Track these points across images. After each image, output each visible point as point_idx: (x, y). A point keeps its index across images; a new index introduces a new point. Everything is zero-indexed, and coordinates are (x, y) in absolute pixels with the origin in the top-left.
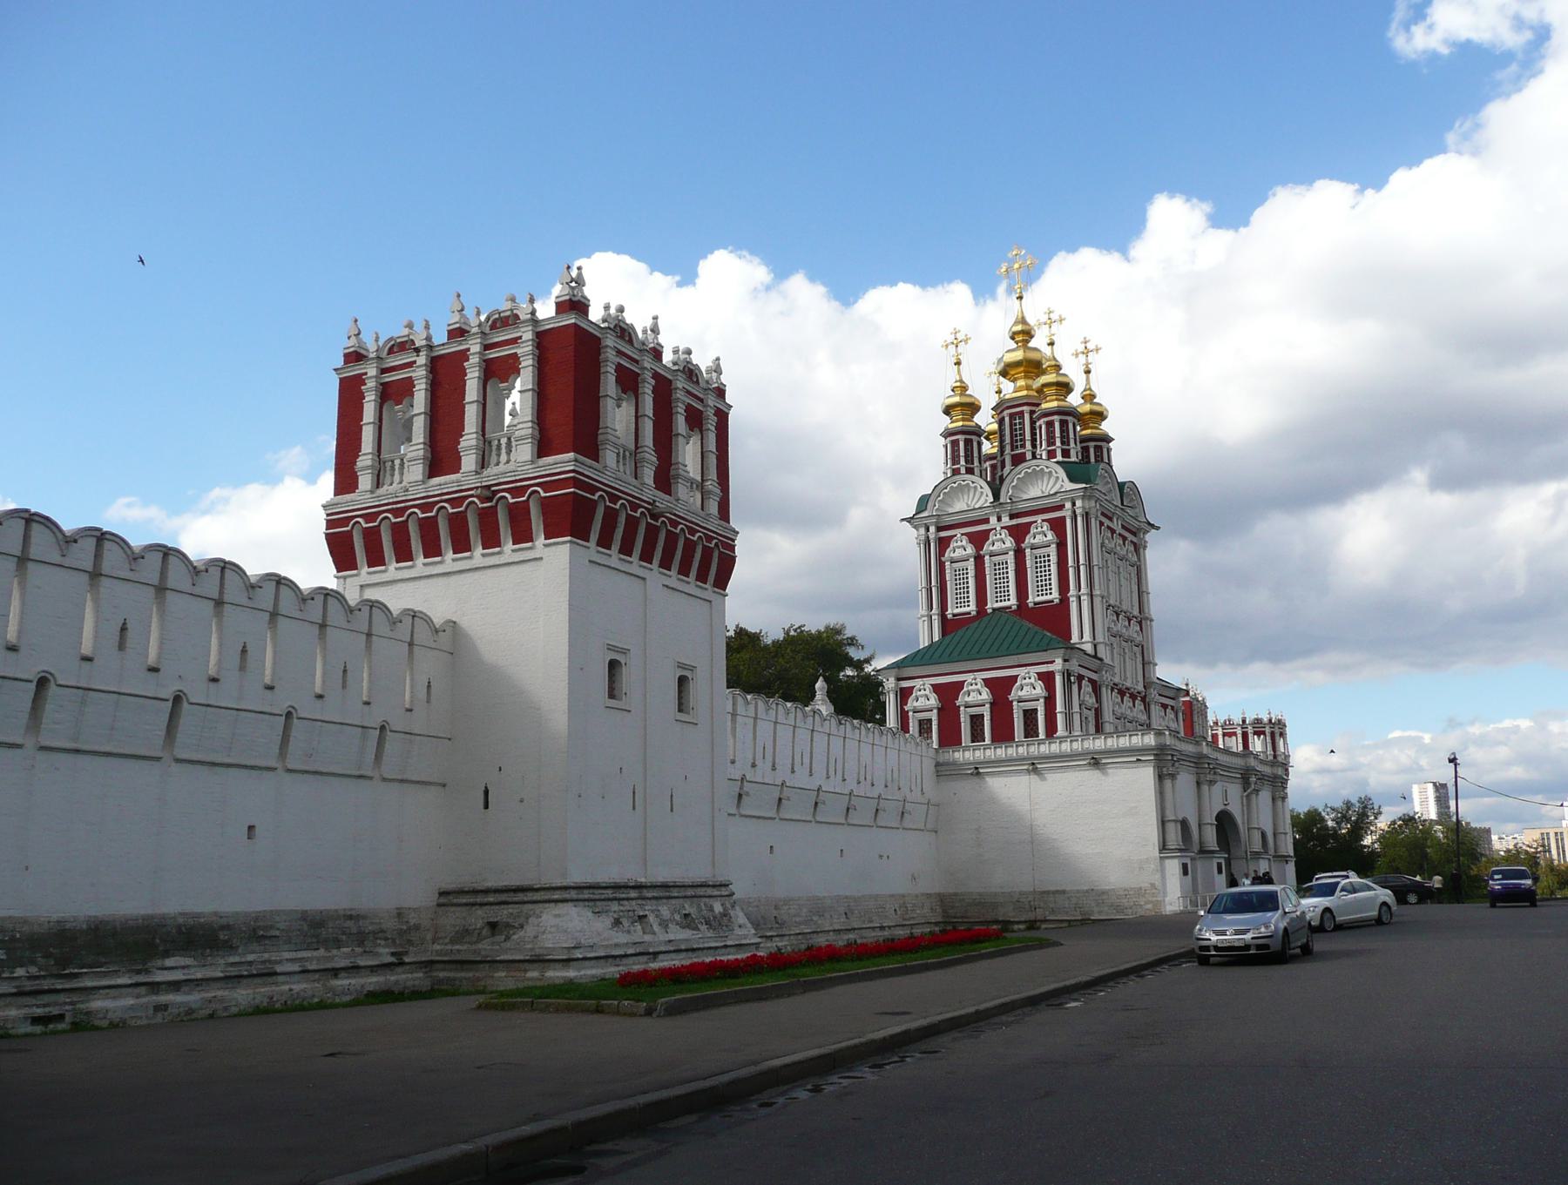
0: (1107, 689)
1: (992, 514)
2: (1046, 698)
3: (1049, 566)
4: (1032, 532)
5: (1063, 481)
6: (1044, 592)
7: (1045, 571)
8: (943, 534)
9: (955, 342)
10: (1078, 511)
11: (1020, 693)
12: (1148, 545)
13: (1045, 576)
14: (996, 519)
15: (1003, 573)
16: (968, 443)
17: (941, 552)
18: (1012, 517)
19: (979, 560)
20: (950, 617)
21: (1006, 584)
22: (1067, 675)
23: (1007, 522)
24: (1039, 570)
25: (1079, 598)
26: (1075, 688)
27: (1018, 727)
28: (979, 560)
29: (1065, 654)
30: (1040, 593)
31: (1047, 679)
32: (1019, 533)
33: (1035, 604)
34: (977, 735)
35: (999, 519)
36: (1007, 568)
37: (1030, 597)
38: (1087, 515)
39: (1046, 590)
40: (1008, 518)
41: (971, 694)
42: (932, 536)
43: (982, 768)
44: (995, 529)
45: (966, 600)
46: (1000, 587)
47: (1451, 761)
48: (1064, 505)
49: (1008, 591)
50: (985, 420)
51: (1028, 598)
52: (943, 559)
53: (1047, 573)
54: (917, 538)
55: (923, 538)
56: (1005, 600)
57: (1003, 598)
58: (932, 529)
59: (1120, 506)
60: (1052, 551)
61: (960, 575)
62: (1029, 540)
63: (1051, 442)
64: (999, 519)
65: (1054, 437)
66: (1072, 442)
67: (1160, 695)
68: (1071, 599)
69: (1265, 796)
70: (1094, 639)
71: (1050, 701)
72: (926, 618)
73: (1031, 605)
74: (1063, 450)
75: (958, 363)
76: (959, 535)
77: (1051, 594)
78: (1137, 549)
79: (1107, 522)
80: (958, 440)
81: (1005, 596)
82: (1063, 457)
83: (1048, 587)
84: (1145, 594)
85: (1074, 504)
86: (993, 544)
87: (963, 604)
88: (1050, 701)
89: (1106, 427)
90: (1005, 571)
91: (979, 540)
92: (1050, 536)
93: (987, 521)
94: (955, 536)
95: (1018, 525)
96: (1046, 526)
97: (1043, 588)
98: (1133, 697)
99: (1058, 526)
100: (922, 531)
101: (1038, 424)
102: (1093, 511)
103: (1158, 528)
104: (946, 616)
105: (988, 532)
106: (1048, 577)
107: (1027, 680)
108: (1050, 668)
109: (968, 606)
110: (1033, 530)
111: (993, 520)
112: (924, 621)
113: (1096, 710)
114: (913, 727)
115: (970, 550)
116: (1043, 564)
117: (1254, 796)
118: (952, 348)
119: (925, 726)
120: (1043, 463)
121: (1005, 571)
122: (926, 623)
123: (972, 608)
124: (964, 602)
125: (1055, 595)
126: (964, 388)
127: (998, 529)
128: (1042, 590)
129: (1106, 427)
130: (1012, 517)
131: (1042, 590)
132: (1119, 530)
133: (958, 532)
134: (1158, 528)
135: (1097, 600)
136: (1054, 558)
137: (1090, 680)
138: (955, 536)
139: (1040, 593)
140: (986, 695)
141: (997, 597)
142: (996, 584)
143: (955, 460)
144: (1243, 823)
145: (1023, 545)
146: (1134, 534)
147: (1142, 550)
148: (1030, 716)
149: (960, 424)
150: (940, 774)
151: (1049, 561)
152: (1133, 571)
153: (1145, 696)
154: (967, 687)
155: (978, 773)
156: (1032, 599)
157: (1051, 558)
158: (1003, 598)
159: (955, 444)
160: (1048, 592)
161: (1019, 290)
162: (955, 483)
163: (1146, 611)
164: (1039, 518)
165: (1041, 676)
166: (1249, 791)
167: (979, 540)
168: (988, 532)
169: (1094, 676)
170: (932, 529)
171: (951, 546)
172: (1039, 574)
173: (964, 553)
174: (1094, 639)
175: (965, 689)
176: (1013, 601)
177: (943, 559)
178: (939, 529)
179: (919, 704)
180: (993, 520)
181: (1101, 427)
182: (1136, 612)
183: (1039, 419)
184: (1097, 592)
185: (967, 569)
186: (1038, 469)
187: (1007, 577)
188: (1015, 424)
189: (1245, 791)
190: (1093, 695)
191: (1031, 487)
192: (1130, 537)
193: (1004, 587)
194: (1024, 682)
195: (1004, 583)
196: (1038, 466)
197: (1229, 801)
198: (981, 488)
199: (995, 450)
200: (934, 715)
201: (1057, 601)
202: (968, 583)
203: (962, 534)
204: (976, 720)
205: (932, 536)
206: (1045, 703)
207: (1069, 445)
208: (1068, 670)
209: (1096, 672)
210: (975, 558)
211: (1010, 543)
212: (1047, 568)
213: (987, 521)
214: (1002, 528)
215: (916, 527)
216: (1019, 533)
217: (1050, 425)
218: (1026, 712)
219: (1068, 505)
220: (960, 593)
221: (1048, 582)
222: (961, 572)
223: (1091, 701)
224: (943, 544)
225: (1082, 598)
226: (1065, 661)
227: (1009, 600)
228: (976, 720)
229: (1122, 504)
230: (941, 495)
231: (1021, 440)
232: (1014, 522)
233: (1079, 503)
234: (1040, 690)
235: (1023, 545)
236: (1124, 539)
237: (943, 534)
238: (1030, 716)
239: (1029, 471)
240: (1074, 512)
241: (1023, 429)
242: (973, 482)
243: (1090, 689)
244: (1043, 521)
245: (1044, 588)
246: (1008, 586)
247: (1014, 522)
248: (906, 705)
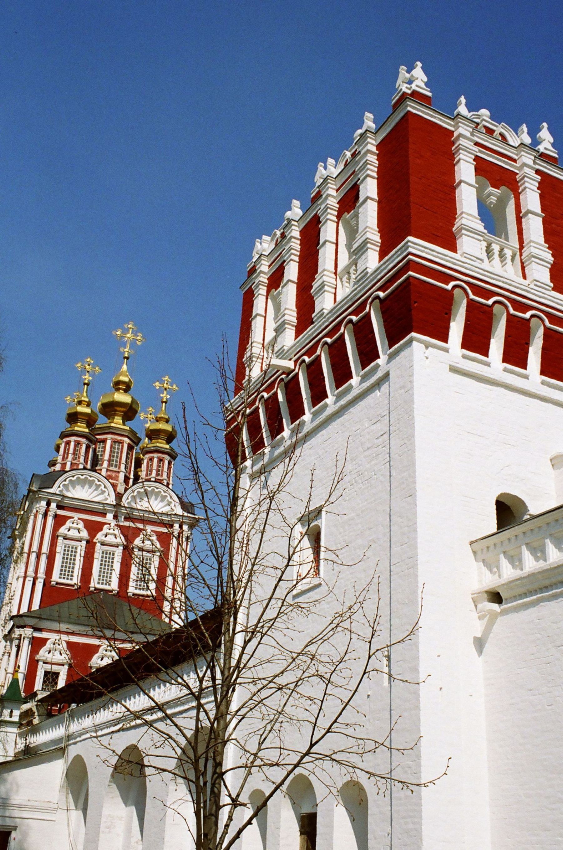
1: (110, 512)
8: (61, 512)
17: (56, 528)
44: (110, 524)
58: (53, 505)
61: (69, 554)
76: (76, 518)
93: (104, 515)
94: (73, 518)
99: (165, 539)
105: (102, 524)
111: (110, 516)
127: (113, 524)
138: (73, 518)
162: (82, 475)
168: (102, 524)
170: (53, 505)
173: (78, 534)
178: (59, 507)
180: (110, 516)
186: (156, 490)
198: (105, 487)
203: (79, 519)
219: (176, 526)
232: (127, 524)
237: (61, 512)
247: (127, 524)
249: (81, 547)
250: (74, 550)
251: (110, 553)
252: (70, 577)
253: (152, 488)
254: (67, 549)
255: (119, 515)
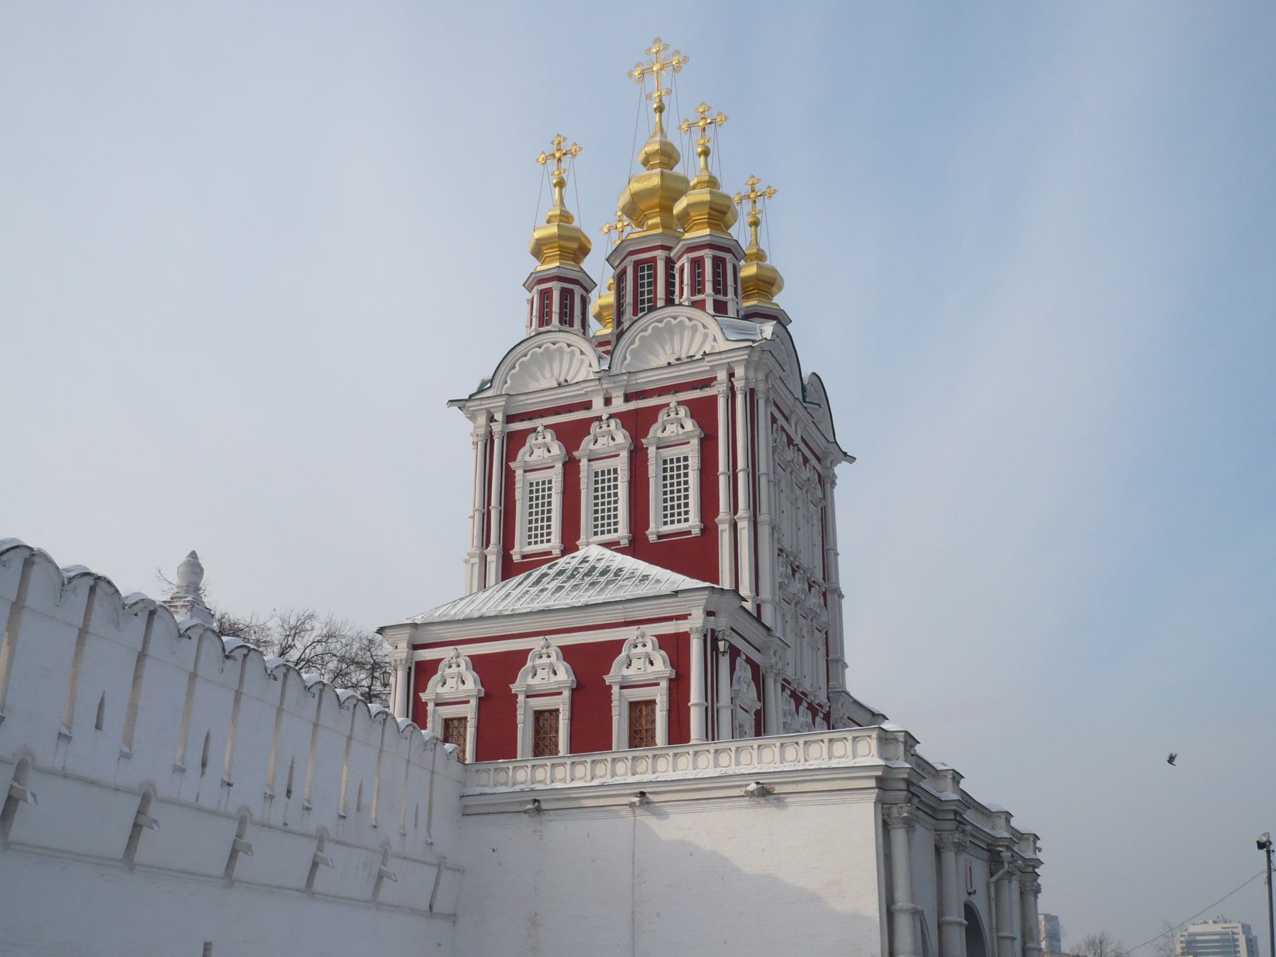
0: (775, 681)
2: (671, 680)
3: (686, 475)
4: (660, 420)
5: (715, 340)
6: (676, 518)
7: (679, 483)
9: (557, 155)
10: (739, 384)
11: (626, 672)
12: (837, 481)
13: (679, 491)
14: (601, 401)
15: (609, 488)
16: (566, 295)
18: (628, 398)
19: (571, 467)
20: (516, 558)
21: (612, 506)
22: (711, 639)
23: (620, 406)
24: (668, 482)
25: (735, 527)
26: (724, 662)
27: (618, 738)
28: (571, 467)
29: (708, 602)
30: (669, 519)
31: (675, 647)
32: (637, 424)
33: (660, 537)
34: (544, 745)
35: (608, 401)
36: (616, 479)
37: (652, 524)
38: (751, 394)
39: (679, 514)
40: (622, 399)
41: (539, 672)
42: (497, 428)
43: (547, 801)
45: (545, 531)
46: (603, 511)
47: (1261, 845)
48: (716, 377)
49: (615, 516)
50: (597, 268)
51: (647, 527)
52: (512, 465)
53: (682, 487)
54: (472, 434)
55: (482, 431)
56: (609, 531)
57: (606, 528)
58: (499, 416)
59: (801, 401)
60: (692, 452)
62: (655, 431)
63: (697, 287)
64: (608, 401)
65: (702, 283)
66: (730, 290)
67: (849, 718)
68: (721, 527)
69: (1012, 890)
70: (757, 594)
71: (678, 687)
72: (476, 560)
73: (652, 538)
74: (716, 302)
75: (561, 184)
77: (686, 520)
78: (821, 480)
79: (781, 421)
80: (549, 291)
81: (609, 524)
82: (714, 310)
83: (683, 510)
84: (832, 553)
85: (731, 375)
86: (596, 441)
87: (539, 539)
88: (678, 687)
89: (781, 300)
90: (612, 484)
91: (572, 435)
92: (690, 425)
93: (587, 405)
95: (637, 412)
96: (683, 411)
97: (674, 509)
98: (814, 710)
99: (703, 412)
100: (482, 420)
101: (677, 266)
102: (761, 388)
103: (852, 459)
104: (511, 556)
106: (682, 494)
107: (640, 649)
108: (682, 626)
109: (549, 541)
110: (662, 416)
111: (598, 403)
112: (473, 565)
113: (758, 713)
114: (433, 729)
115: (557, 449)
116: (675, 473)
117: (1006, 882)
118: (552, 164)
119: (451, 728)
120: (683, 312)
121: (612, 484)
122: (476, 568)
123: (555, 544)
124: (542, 535)
125: (693, 523)
126: (565, 217)
128: (672, 515)
129: (781, 300)
130: (628, 398)
131: (672, 515)
132: (797, 440)
133: (539, 423)
134: (852, 459)
135: (764, 531)
136: (694, 463)
137: (749, 660)
139: (669, 519)
140: (564, 675)
141: (596, 526)
142: (596, 505)
143: (544, 319)
144: (991, 928)
145: (643, 441)
146: (819, 460)
147: (828, 485)
148: (642, 711)
149: (558, 264)
150: (468, 811)
151: (686, 467)
152: (815, 512)
153: (829, 713)
154: (533, 660)
155: (539, 810)
156: (656, 528)
157: (690, 462)
158: (606, 528)
159: (545, 295)
160: (683, 517)
161: (657, 100)
163: (833, 580)
164: (671, 399)
165: (665, 642)
166: (1000, 873)
167: (572, 435)
169: (755, 656)
171: (527, 444)
172: (668, 489)
174: (757, 594)
175: (529, 664)
176: (622, 533)
177: (512, 465)
178: (510, 419)
179: (447, 691)
180: (598, 403)
181: (773, 301)
182: (819, 576)
183: (679, 258)
184: (763, 517)
185: (550, 482)
186: (674, 322)
187: (616, 495)
188: (642, 277)
189: (992, 875)
190: (753, 685)
191: (659, 348)
192: (814, 462)
193: (609, 510)
194: (634, 651)
195: (609, 503)
196: (675, 318)
197: (974, 888)
198: (582, 353)
199: (608, 331)
200: (469, 711)
201: (696, 532)
202: (549, 504)
204: (543, 720)
205: (497, 428)
206: (670, 689)
207: (725, 294)
208: (713, 631)
209: (759, 651)
210: (565, 464)
211: (622, 437)
212: (682, 479)
213: (587, 405)
214: (611, 416)
215: (472, 417)
216: (637, 424)
217: (697, 264)
218: (633, 705)
219: (722, 375)
220: (537, 521)
221: (682, 502)
222: (540, 487)
223: (749, 694)
224: (515, 442)
225: (739, 526)
226: (710, 614)
227: (616, 530)
228: (543, 720)
229: (804, 397)
230: (517, 365)
231: (649, 300)
233: (739, 372)
234: (661, 667)
235: (643, 441)
236: (806, 460)
238: (642, 711)
239: (660, 325)
240: (732, 389)
241: (653, 283)
242: (569, 346)
243: (749, 673)
244: (680, 403)
245: (676, 511)
246: (616, 509)
247: (632, 405)
248: (424, 691)
249: (556, 475)
250: (547, 486)
251: (609, 471)
252: (545, 538)
253: (665, 321)
254: (534, 488)
255: (613, 395)
